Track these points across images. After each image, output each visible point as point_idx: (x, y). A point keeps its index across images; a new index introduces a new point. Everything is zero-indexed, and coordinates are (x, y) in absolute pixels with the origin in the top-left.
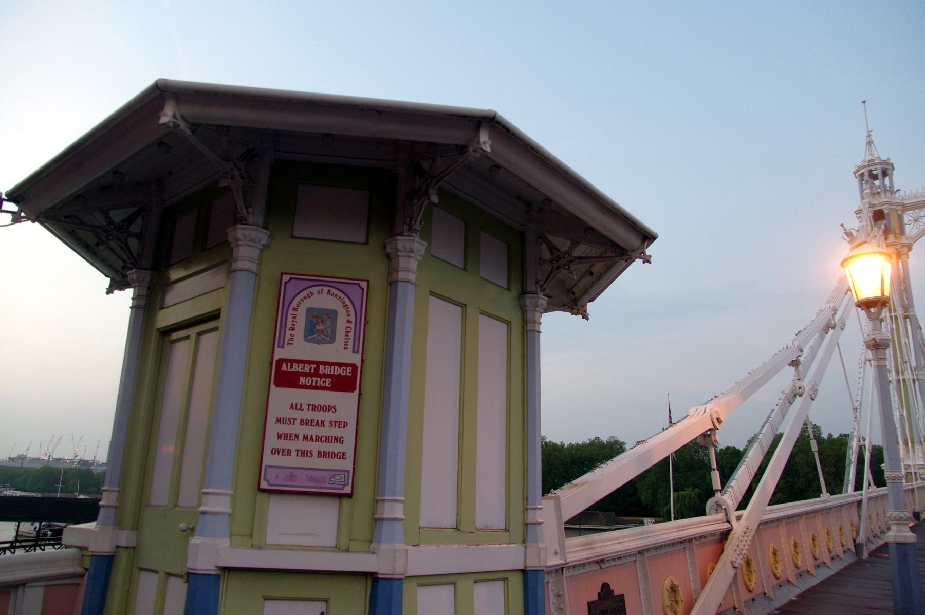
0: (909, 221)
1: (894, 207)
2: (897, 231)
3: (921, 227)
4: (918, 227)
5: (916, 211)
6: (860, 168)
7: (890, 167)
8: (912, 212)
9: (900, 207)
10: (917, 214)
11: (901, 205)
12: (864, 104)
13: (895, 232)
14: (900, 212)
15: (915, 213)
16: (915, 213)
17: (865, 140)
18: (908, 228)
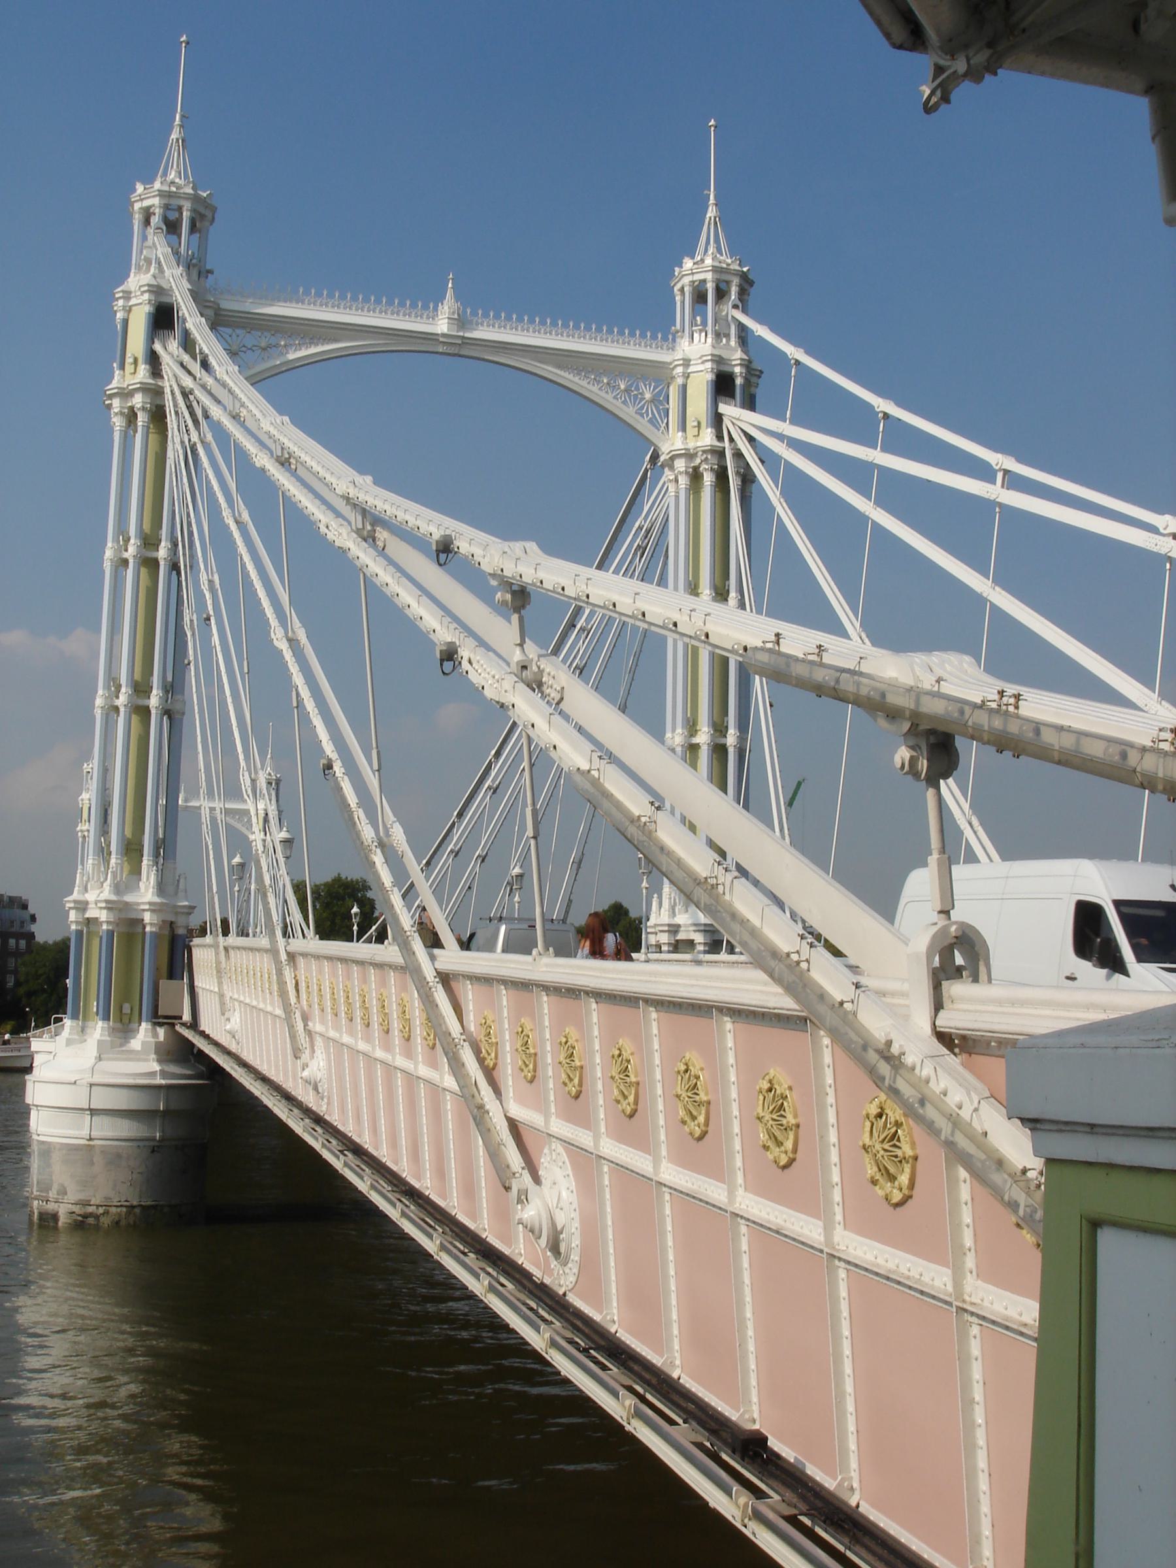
5: (238, 331)
7: (209, 214)
8: (229, 331)
15: (234, 336)
16: (234, 336)
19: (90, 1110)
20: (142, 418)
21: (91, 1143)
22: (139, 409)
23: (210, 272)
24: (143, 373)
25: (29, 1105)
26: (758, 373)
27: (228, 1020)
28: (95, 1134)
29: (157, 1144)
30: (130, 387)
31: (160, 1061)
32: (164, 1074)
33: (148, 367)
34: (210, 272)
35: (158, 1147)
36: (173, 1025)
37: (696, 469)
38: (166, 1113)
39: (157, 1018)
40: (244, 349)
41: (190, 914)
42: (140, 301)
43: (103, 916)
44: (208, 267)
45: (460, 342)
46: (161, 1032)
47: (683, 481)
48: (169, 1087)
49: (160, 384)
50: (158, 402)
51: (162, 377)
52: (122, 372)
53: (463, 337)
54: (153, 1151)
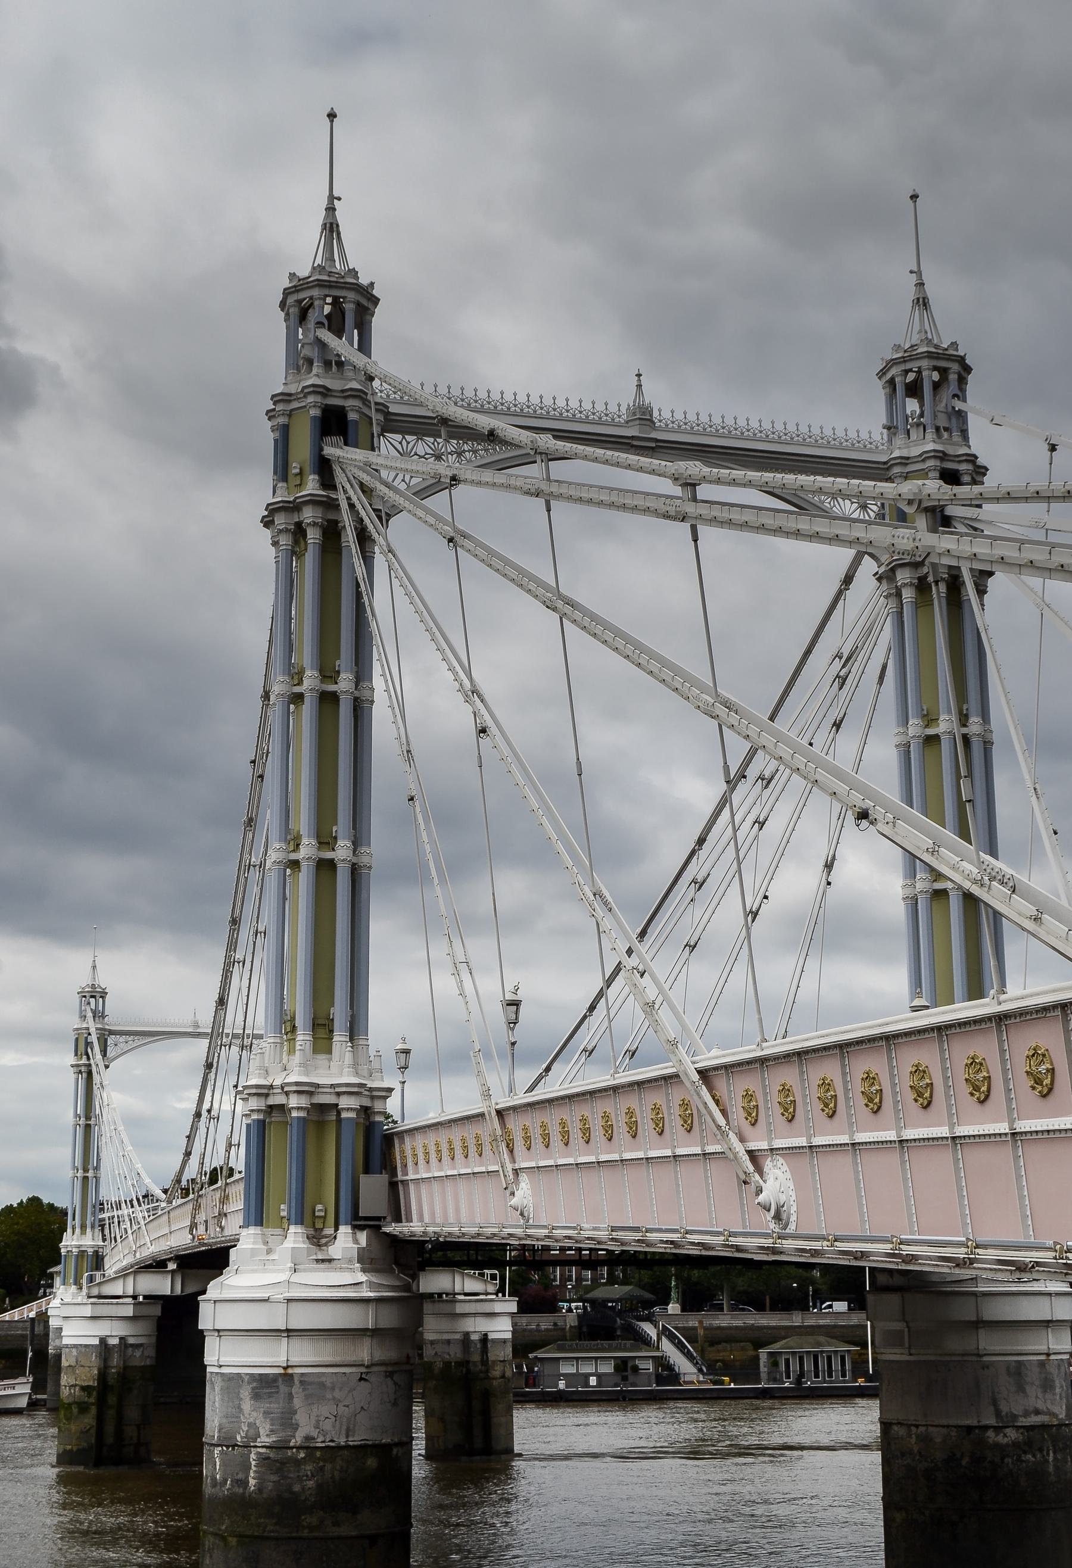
5: (409, 438)
6: (298, 285)
8: (399, 437)
10: (410, 446)
12: (332, 122)
17: (320, 216)
19: (288, 1330)
20: (313, 535)
21: (290, 1371)
22: (309, 524)
24: (312, 486)
25: (202, 1331)
26: (983, 471)
27: (513, 1194)
28: (295, 1360)
29: (364, 1370)
30: (298, 501)
31: (364, 1270)
32: (372, 1285)
33: (317, 477)
35: (367, 1373)
36: (379, 1227)
37: (922, 580)
38: (374, 1333)
39: (358, 1222)
41: (387, 1097)
42: (303, 404)
43: (294, 1101)
45: (653, 445)
46: (363, 1237)
47: (908, 594)
48: (378, 1300)
49: (334, 496)
50: (331, 516)
51: (334, 488)
52: (285, 485)
53: (656, 440)
54: (361, 1379)
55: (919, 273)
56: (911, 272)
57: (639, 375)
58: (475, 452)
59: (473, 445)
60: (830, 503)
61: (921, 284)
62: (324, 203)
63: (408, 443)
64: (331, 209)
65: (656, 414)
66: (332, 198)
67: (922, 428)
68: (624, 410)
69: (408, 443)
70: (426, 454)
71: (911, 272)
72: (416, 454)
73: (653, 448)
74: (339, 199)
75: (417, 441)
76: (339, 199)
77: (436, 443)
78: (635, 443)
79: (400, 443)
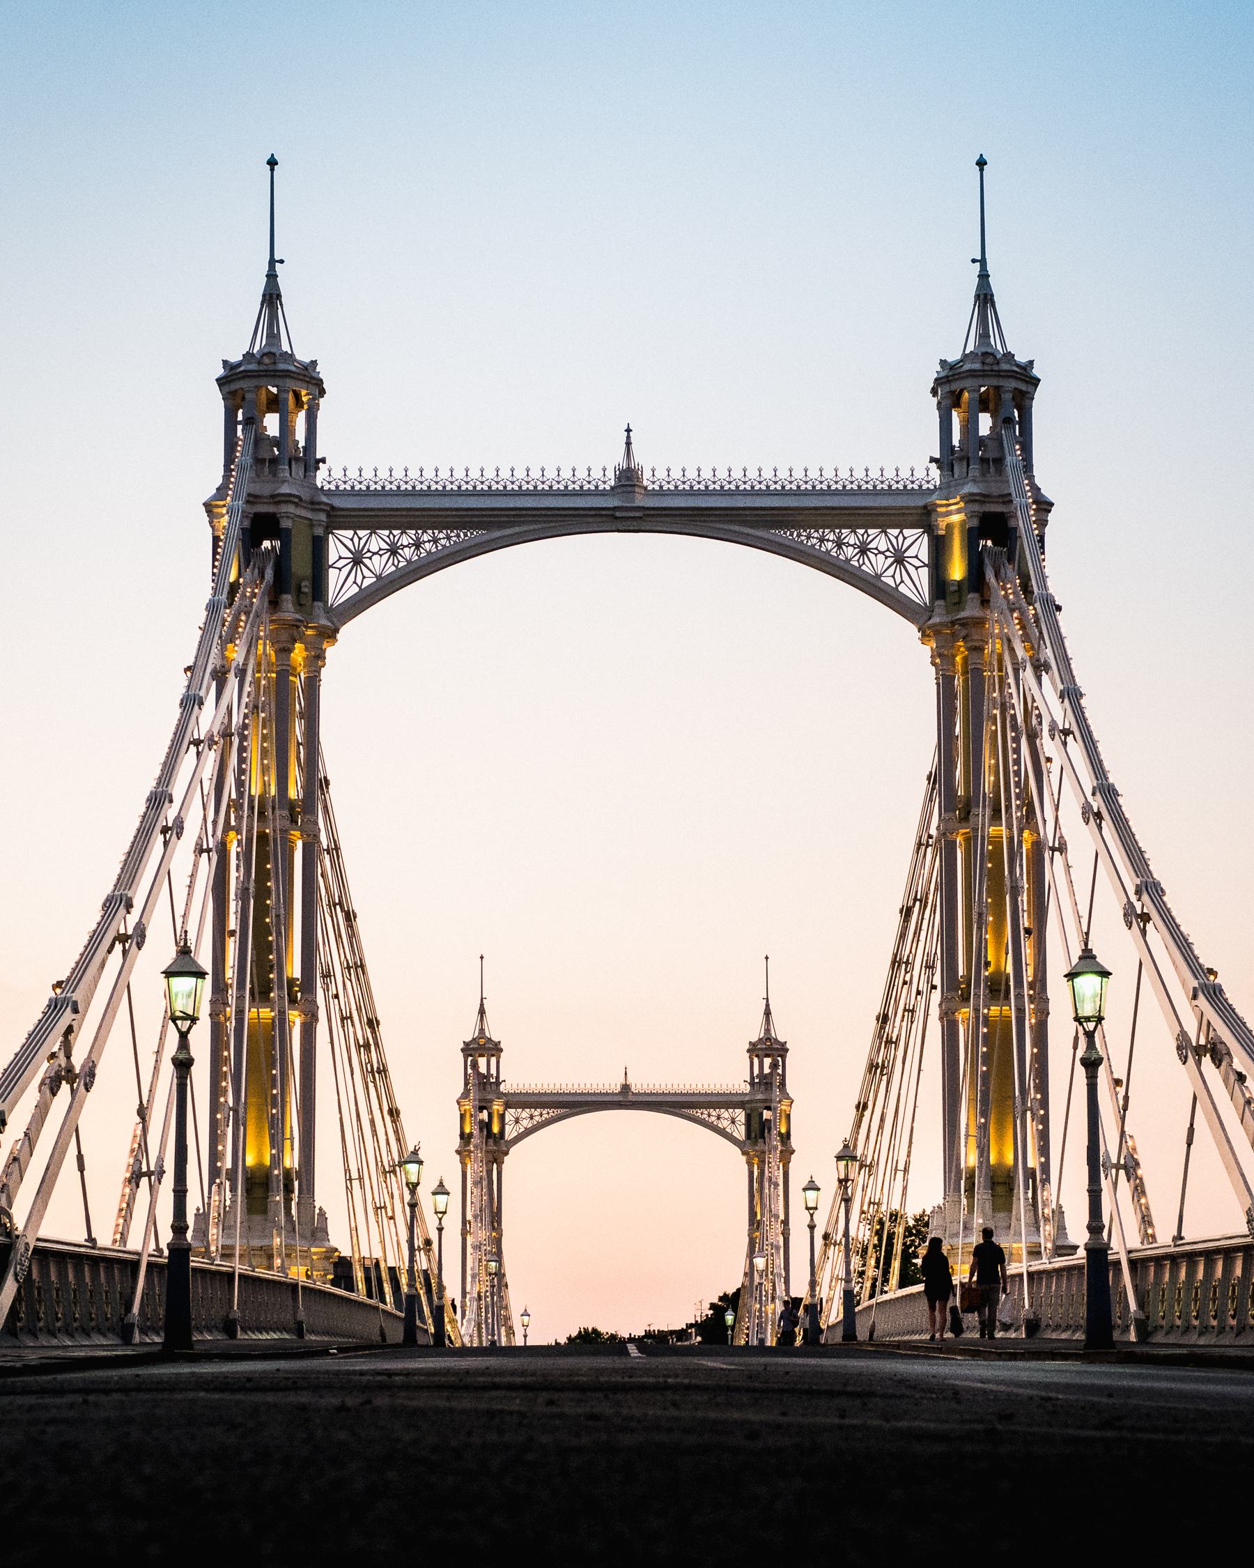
0: (340, 558)
1: (309, 515)
2: (306, 587)
3: (367, 583)
4: (359, 581)
8: (350, 533)
9: (323, 517)
11: (324, 510)
13: (299, 588)
14: (319, 531)
15: (356, 540)
16: (356, 540)
18: (334, 578)
23: (323, 460)
26: (1046, 507)
34: (323, 460)
40: (369, 555)
44: (319, 456)
55: (983, 262)
56: (974, 261)
57: (628, 430)
58: (435, 541)
59: (434, 533)
60: (858, 561)
61: (984, 277)
62: (265, 268)
63: (360, 539)
64: (272, 277)
65: (647, 475)
66: (272, 262)
67: (965, 463)
68: (611, 475)
69: (360, 539)
70: (380, 549)
71: (974, 261)
72: (369, 551)
73: (640, 518)
74: (282, 262)
75: (371, 535)
76: (282, 262)
77: (391, 537)
78: (618, 514)
79: (352, 540)
